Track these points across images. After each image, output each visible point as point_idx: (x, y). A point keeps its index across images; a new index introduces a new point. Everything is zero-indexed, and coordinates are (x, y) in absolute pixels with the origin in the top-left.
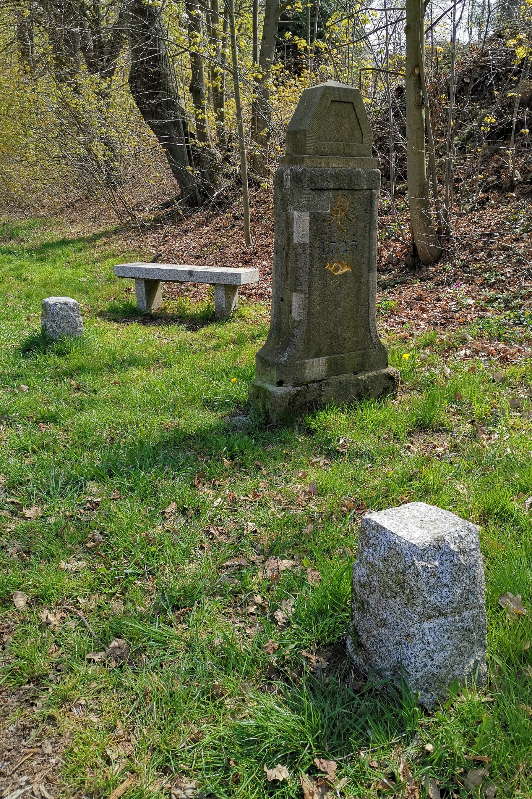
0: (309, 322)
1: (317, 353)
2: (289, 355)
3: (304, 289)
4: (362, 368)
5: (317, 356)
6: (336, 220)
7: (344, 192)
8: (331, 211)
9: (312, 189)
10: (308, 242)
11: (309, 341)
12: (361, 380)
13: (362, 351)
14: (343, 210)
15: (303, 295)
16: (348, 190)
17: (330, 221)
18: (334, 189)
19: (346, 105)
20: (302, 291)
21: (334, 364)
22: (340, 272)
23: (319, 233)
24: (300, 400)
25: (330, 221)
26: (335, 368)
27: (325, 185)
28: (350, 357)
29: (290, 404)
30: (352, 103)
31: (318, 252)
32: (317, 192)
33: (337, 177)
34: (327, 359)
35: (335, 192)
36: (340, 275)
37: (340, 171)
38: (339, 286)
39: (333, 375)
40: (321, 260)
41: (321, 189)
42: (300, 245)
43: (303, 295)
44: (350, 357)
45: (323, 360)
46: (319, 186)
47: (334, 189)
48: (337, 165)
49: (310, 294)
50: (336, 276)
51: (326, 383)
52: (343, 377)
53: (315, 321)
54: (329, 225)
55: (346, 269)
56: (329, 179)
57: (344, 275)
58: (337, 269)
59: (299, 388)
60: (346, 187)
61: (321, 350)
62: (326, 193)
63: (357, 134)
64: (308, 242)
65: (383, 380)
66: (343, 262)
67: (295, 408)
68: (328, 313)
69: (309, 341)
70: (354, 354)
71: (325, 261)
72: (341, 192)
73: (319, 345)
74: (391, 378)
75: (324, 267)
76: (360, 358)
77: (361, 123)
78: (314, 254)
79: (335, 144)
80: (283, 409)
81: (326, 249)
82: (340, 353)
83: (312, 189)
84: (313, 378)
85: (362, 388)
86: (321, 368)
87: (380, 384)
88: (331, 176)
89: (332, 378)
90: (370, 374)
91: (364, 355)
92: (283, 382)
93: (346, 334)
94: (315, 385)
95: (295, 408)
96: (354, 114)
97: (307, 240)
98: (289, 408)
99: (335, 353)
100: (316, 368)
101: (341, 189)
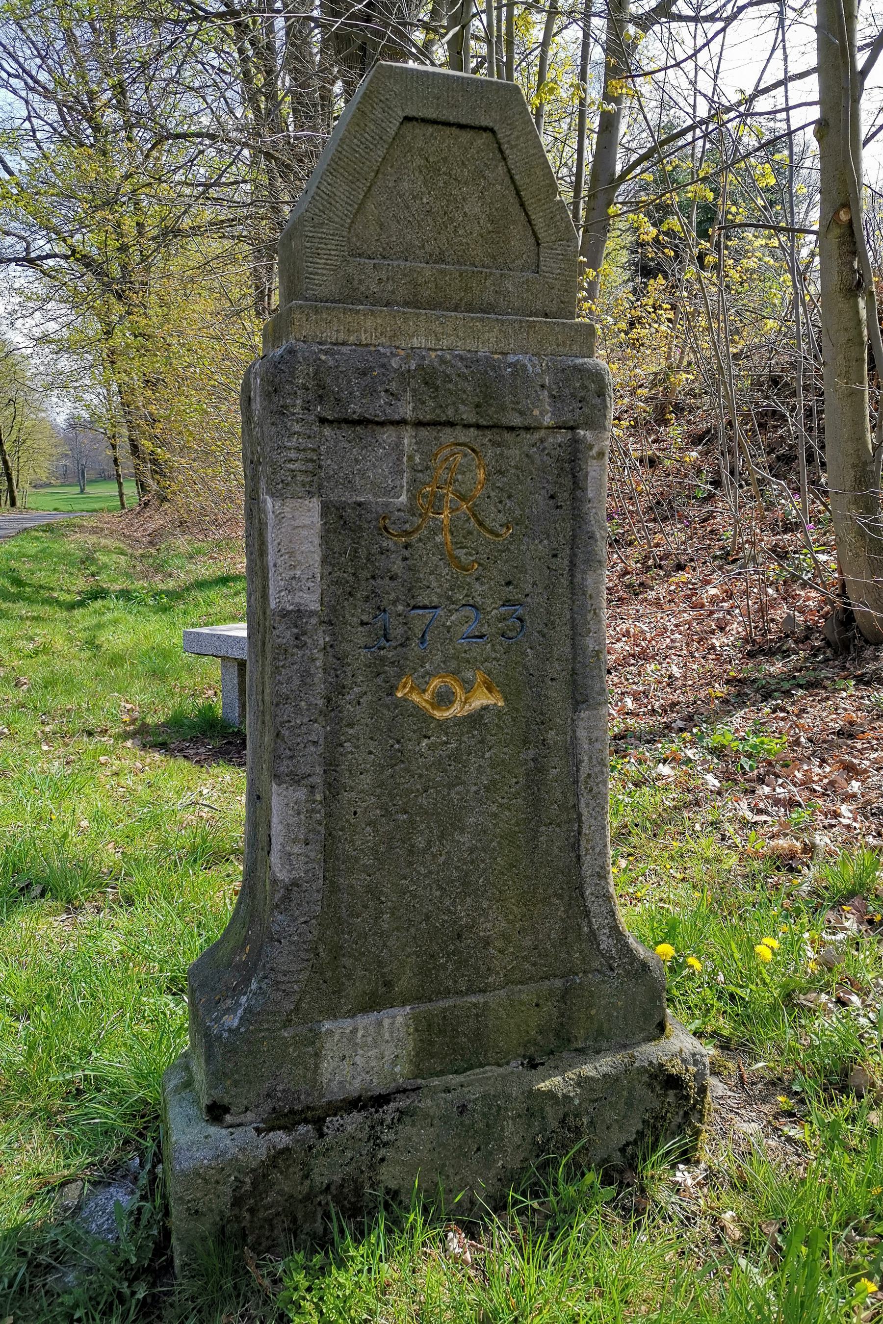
0: (333, 888)
1: (373, 994)
2: (249, 1010)
3: (304, 770)
4: (557, 1043)
5: (372, 1003)
6: (434, 532)
7: (464, 436)
8: (412, 498)
9: (323, 421)
10: (315, 606)
11: (336, 952)
12: (550, 1095)
13: (558, 983)
14: (463, 498)
15: (301, 794)
16: (478, 427)
17: (407, 533)
18: (419, 424)
19: (465, 136)
20: (296, 779)
21: (442, 1032)
22: (456, 710)
23: (365, 574)
24: (287, 1184)
25: (407, 533)
26: (446, 1046)
27: (378, 407)
28: (511, 1007)
29: (237, 1202)
30: (492, 131)
31: (361, 641)
32: (348, 432)
33: (429, 379)
34: (415, 1018)
35: (424, 432)
36: (459, 722)
37: (442, 360)
38: (455, 756)
39: (442, 1073)
40: (376, 668)
41: (363, 422)
42: (284, 614)
43: (301, 794)
44: (511, 1007)
45: (398, 1020)
46: (355, 409)
47: (419, 424)
48: (427, 338)
49: (333, 788)
50: (442, 725)
51: (402, 1112)
52: (476, 1084)
53: (359, 880)
54: (406, 546)
55: (481, 699)
56: (393, 387)
57: (476, 719)
58: (444, 699)
59: (281, 1139)
60: (469, 416)
61: (387, 984)
62: (388, 435)
63: (518, 239)
64: (315, 606)
65: (641, 1090)
66: (469, 675)
67: (262, 1214)
68: (411, 852)
69: (336, 952)
70: (526, 993)
71: (391, 671)
72: (448, 436)
73: (380, 964)
74: (674, 1082)
75: (391, 694)
76: (550, 1008)
77: (529, 201)
78: (346, 646)
79: (428, 271)
80: (205, 1227)
81: (398, 632)
82: (470, 991)
83: (323, 421)
84: (355, 1087)
85: (554, 1124)
86: (389, 1051)
87: (629, 1104)
88: (404, 376)
89: (436, 1082)
90: (587, 1070)
91: (565, 995)
92: (226, 1110)
93: (493, 925)
94: (353, 1121)
95: (262, 1214)
96: (501, 169)
97: (311, 601)
98: (238, 1219)
99: (447, 993)
100: (365, 1049)
101: (451, 424)
